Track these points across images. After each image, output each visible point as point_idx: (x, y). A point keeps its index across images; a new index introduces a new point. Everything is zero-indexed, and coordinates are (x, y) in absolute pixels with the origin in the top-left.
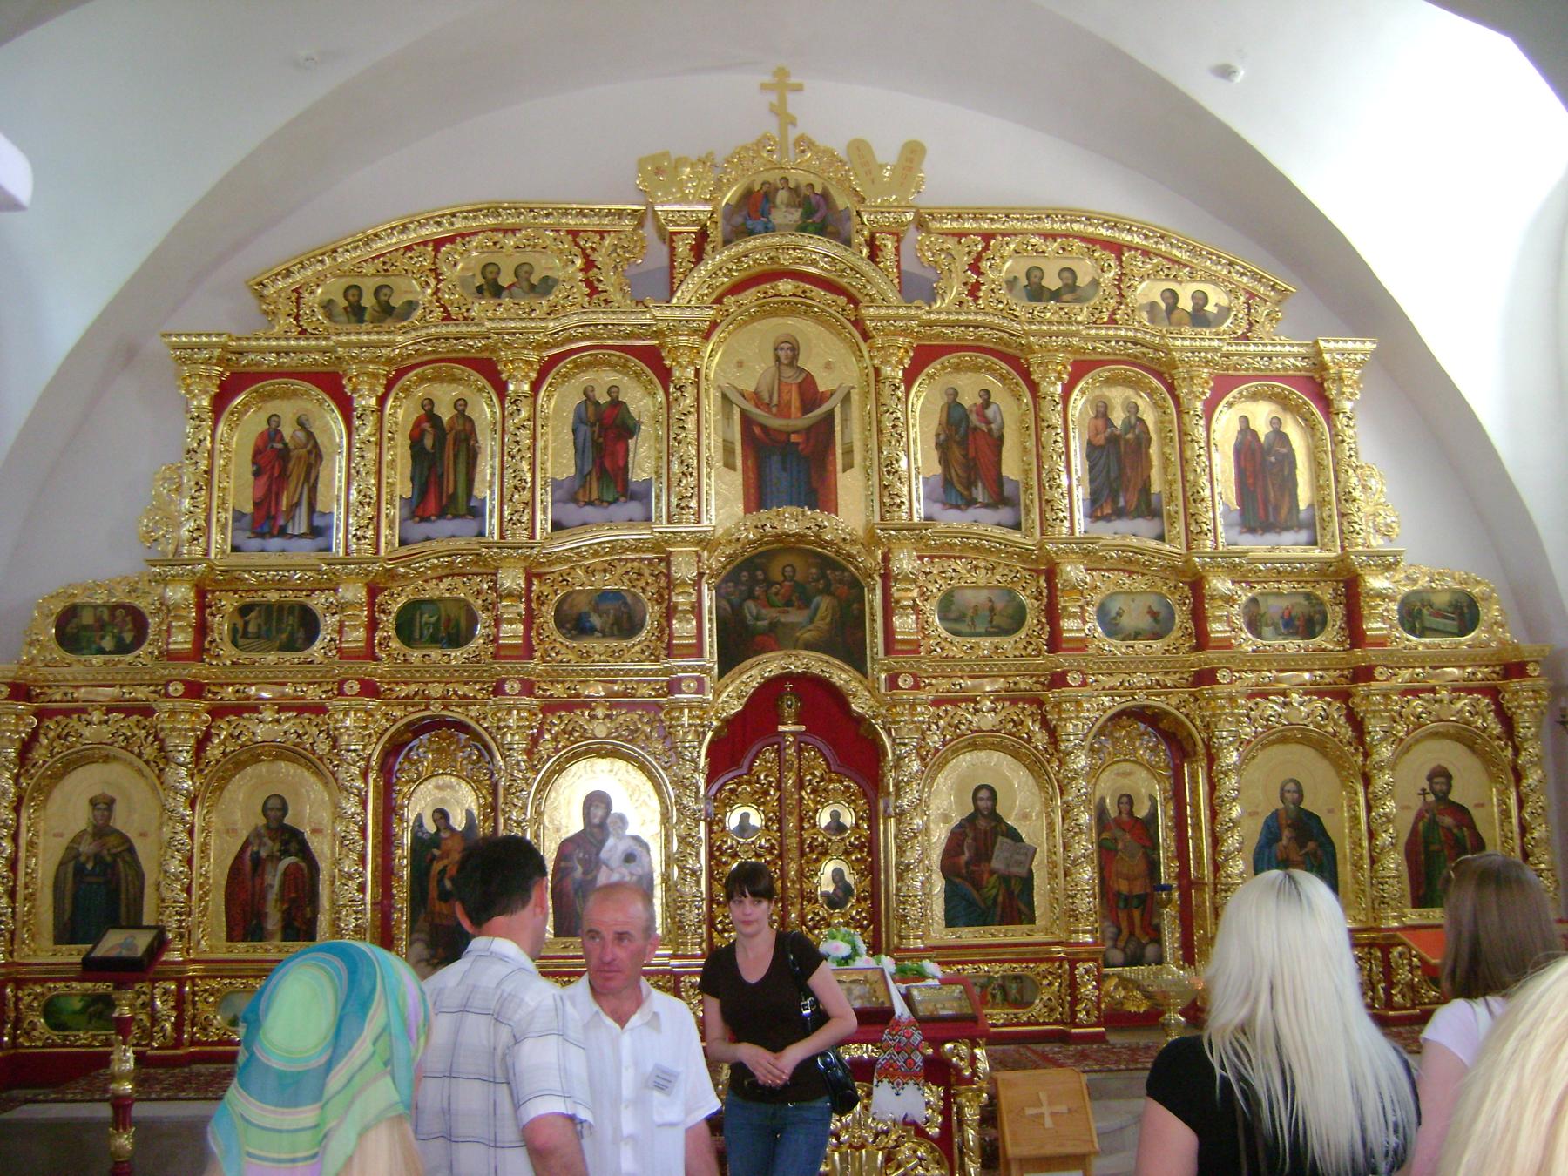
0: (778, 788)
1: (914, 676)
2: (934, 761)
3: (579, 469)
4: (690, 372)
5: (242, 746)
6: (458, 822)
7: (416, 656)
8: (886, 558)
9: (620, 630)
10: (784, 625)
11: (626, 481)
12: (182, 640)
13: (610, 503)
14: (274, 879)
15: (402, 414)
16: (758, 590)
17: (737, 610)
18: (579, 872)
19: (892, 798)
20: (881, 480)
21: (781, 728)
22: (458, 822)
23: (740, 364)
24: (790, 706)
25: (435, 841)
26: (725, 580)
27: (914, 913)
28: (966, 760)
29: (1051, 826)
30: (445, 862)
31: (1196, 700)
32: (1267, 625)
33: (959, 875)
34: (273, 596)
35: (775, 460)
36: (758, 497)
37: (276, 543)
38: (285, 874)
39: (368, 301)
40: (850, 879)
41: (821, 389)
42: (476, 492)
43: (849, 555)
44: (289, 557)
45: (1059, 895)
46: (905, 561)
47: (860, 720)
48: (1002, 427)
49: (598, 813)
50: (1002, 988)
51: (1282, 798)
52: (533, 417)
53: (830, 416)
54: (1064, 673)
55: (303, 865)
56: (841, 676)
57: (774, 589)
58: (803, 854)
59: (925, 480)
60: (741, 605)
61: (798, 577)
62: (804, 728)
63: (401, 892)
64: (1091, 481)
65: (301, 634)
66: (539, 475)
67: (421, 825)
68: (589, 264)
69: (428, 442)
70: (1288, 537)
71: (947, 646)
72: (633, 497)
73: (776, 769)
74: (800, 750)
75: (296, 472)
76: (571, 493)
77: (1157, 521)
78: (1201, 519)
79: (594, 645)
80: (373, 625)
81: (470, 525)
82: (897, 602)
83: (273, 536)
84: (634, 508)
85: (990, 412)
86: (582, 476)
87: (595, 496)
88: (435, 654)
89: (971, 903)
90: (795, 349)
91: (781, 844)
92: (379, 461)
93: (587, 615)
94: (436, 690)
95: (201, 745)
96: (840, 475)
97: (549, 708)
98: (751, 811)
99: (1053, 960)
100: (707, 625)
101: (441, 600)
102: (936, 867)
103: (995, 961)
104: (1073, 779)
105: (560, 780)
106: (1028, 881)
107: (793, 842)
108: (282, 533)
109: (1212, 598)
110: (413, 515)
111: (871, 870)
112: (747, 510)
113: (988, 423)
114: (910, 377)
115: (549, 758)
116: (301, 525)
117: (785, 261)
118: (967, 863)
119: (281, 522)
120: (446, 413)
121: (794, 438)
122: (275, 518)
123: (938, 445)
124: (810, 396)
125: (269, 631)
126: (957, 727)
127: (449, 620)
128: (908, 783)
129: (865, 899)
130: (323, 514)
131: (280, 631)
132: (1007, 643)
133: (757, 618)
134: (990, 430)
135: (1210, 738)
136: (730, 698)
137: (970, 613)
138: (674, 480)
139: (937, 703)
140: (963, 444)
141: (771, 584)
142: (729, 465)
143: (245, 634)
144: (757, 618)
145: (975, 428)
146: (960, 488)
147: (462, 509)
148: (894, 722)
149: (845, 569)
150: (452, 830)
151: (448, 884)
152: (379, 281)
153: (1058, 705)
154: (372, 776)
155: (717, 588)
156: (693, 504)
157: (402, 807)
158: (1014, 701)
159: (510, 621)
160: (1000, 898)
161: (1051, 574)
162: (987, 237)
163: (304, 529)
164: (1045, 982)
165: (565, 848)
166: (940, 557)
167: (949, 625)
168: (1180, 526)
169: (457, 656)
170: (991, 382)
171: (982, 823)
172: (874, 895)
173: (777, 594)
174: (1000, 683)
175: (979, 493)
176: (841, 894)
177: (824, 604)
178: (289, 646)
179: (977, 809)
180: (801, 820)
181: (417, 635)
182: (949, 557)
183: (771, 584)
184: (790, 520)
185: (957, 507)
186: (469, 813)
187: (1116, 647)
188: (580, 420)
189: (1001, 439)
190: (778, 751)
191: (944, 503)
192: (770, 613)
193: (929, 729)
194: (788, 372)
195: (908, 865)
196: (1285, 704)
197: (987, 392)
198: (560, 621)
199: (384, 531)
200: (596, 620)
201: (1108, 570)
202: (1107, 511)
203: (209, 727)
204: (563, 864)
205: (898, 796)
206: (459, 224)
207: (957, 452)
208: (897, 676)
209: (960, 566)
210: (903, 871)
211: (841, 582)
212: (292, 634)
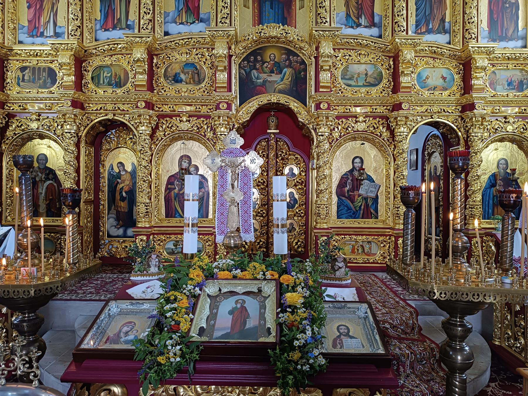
1: (329, 104)
2: (335, 144)
3: (177, 8)
5: (23, 130)
6: (129, 168)
7: (101, 92)
8: (317, 49)
9: (194, 81)
10: (270, 82)
13: (191, 24)
14: (42, 190)
16: (258, 66)
17: (248, 74)
18: (176, 191)
19: (315, 161)
20: (316, 11)
21: (269, 131)
22: (129, 168)
24: (273, 121)
25: (119, 176)
26: (243, 60)
27: (323, 212)
28: (350, 145)
29: (388, 176)
30: (123, 185)
31: (462, 119)
32: (499, 85)
33: (344, 196)
35: (268, 4)
37: (39, 40)
38: (47, 188)
40: (296, 196)
42: (130, 18)
43: (301, 48)
45: (391, 206)
46: (326, 48)
47: (302, 127)
49: (185, 165)
50: (362, 246)
51: (498, 166)
54: (401, 104)
55: (55, 184)
56: (294, 105)
57: (265, 65)
62: (278, 131)
63: (104, 197)
64: (417, 16)
65: (49, 80)
66: (157, 8)
67: (113, 169)
70: (511, 44)
71: (344, 91)
73: (266, 149)
74: (277, 142)
77: (447, 35)
78: (471, 31)
79: (183, 87)
80: (79, 76)
82: (322, 67)
83: (37, 37)
87: (184, 20)
88: (110, 90)
89: (349, 209)
91: (268, 182)
93: (179, 74)
94: (110, 107)
97: (161, 116)
99: (386, 236)
100: (233, 80)
102: (334, 191)
103: (359, 235)
104: (402, 154)
105: (169, 150)
106: (376, 199)
108: (42, 35)
109: (477, 68)
110: (102, 28)
111: (306, 193)
112: (254, 25)
115: (162, 139)
116: (50, 32)
118: (348, 191)
119: (42, 30)
122: (38, 27)
125: (35, 79)
126: (347, 129)
127: (116, 75)
128: (323, 153)
129: (302, 205)
130: (60, 27)
131: (39, 79)
132: (374, 91)
133: (258, 78)
135: (468, 137)
137: (356, 76)
138: (219, 11)
139: (338, 117)
141: (264, 63)
143: (23, 80)
146: (354, 18)
147: (124, 26)
148: (318, 125)
150: (126, 171)
151: (124, 194)
153: (396, 118)
154: (82, 144)
156: (228, 21)
157: (104, 161)
158: (375, 118)
159: (141, 74)
160: (362, 207)
161: (396, 58)
163: (52, 33)
164: (382, 245)
165: (171, 181)
166: (343, 49)
168: (460, 37)
171: (356, 173)
172: (306, 203)
173: (266, 67)
174: (369, 109)
175: (363, 21)
176: (292, 202)
177: (288, 71)
178: (44, 86)
179: (354, 167)
180: (277, 171)
181: (102, 82)
182: (347, 49)
185: (352, 27)
186: (133, 164)
187: (426, 94)
190: (268, 142)
191: (346, 26)
192: (264, 76)
193: (334, 129)
195: (322, 190)
196: (505, 122)
198: (166, 76)
199: (86, 34)
200: (183, 76)
201: (423, 57)
202: (423, 30)
203: (7, 123)
204: (169, 186)
205: (318, 160)
208: (320, 103)
209: (352, 53)
210: (319, 193)
211: (297, 62)
212: (45, 81)
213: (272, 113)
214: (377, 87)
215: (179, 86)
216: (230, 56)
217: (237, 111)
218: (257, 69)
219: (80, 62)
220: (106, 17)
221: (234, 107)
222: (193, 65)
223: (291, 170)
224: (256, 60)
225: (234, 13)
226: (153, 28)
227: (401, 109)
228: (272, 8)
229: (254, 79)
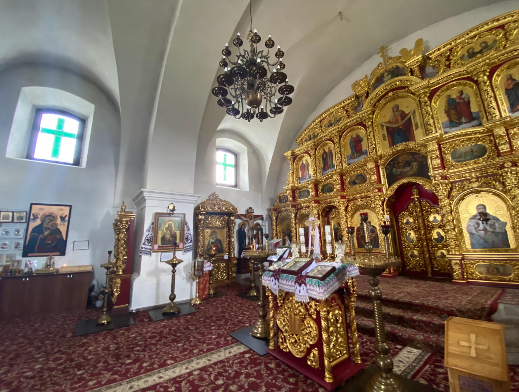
0: (416, 212)
4: (370, 123)
10: (404, 172)
11: (362, 151)
12: (290, 199)
15: (320, 153)
16: (396, 166)
17: (391, 171)
23: (384, 116)
26: (387, 165)
34: (303, 189)
35: (396, 134)
36: (393, 143)
39: (312, 136)
41: (407, 112)
44: (303, 183)
48: (469, 98)
52: (340, 146)
53: (410, 118)
58: (425, 228)
59: (443, 123)
60: (392, 170)
61: (406, 160)
66: (343, 156)
68: (347, 111)
69: (325, 157)
72: (363, 154)
75: (306, 169)
76: (351, 157)
79: (357, 187)
80: (317, 191)
81: (333, 169)
84: (364, 156)
85: (463, 96)
86: (353, 153)
88: (328, 194)
90: (397, 107)
91: (419, 226)
92: (315, 163)
95: (296, 215)
96: (415, 132)
98: (409, 218)
100: (382, 177)
101: (328, 184)
107: (421, 225)
108: (305, 179)
113: (463, 99)
114: (430, 98)
116: (308, 177)
117: (388, 88)
120: (327, 150)
121: (400, 127)
123: (446, 112)
124: (403, 115)
133: (397, 172)
134: (464, 101)
136: (388, 191)
137: (463, 155)
140: (455, 108)
141: (399, 164)
142: (384, 139)
144: (397, 172)
145: (459, 103)
147: (331, 166)
149: (420, 154)
152: (313, 132)
154: (320, 217)
155: (386, 169)
159: (338, 185)
162: (450, 50)
167: (456, 160)
169: (332, 194)
170: (460, 88)
175: (463, 120)
176: (440, 238)
183: (399, 163)
184: (400, 147)
185: (456, 126)
188: (351, 143)
189: (469, 102)
192: (400, 170)
194: (397, 113)
197: (462, 91)
199: (318, 174)
200: (357, 181)
206: (324, 116)
207: (453, 112)
213: (414, 187)
214: (483, 157)
215: (355, 186)
216: (377, 167)
217: (387, 190)
218: (395, 168)
219: (316, 185)
220: (325, 166)
221: (384, 190)
222: (361, 175)
223: (435, 218)
224: (394, 164)
225: (378, 145)
226: (342, 165)
227: (505, 167)
228: (399, 135)
229: (394, 173)
